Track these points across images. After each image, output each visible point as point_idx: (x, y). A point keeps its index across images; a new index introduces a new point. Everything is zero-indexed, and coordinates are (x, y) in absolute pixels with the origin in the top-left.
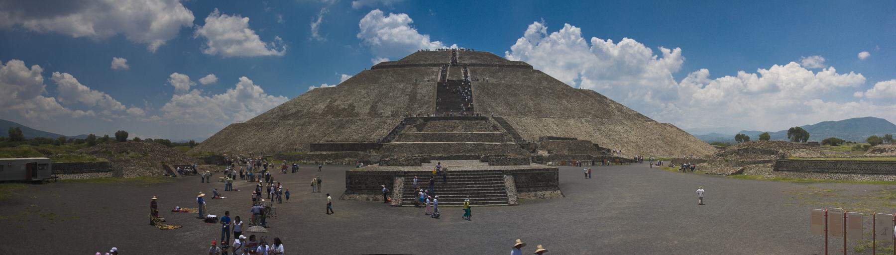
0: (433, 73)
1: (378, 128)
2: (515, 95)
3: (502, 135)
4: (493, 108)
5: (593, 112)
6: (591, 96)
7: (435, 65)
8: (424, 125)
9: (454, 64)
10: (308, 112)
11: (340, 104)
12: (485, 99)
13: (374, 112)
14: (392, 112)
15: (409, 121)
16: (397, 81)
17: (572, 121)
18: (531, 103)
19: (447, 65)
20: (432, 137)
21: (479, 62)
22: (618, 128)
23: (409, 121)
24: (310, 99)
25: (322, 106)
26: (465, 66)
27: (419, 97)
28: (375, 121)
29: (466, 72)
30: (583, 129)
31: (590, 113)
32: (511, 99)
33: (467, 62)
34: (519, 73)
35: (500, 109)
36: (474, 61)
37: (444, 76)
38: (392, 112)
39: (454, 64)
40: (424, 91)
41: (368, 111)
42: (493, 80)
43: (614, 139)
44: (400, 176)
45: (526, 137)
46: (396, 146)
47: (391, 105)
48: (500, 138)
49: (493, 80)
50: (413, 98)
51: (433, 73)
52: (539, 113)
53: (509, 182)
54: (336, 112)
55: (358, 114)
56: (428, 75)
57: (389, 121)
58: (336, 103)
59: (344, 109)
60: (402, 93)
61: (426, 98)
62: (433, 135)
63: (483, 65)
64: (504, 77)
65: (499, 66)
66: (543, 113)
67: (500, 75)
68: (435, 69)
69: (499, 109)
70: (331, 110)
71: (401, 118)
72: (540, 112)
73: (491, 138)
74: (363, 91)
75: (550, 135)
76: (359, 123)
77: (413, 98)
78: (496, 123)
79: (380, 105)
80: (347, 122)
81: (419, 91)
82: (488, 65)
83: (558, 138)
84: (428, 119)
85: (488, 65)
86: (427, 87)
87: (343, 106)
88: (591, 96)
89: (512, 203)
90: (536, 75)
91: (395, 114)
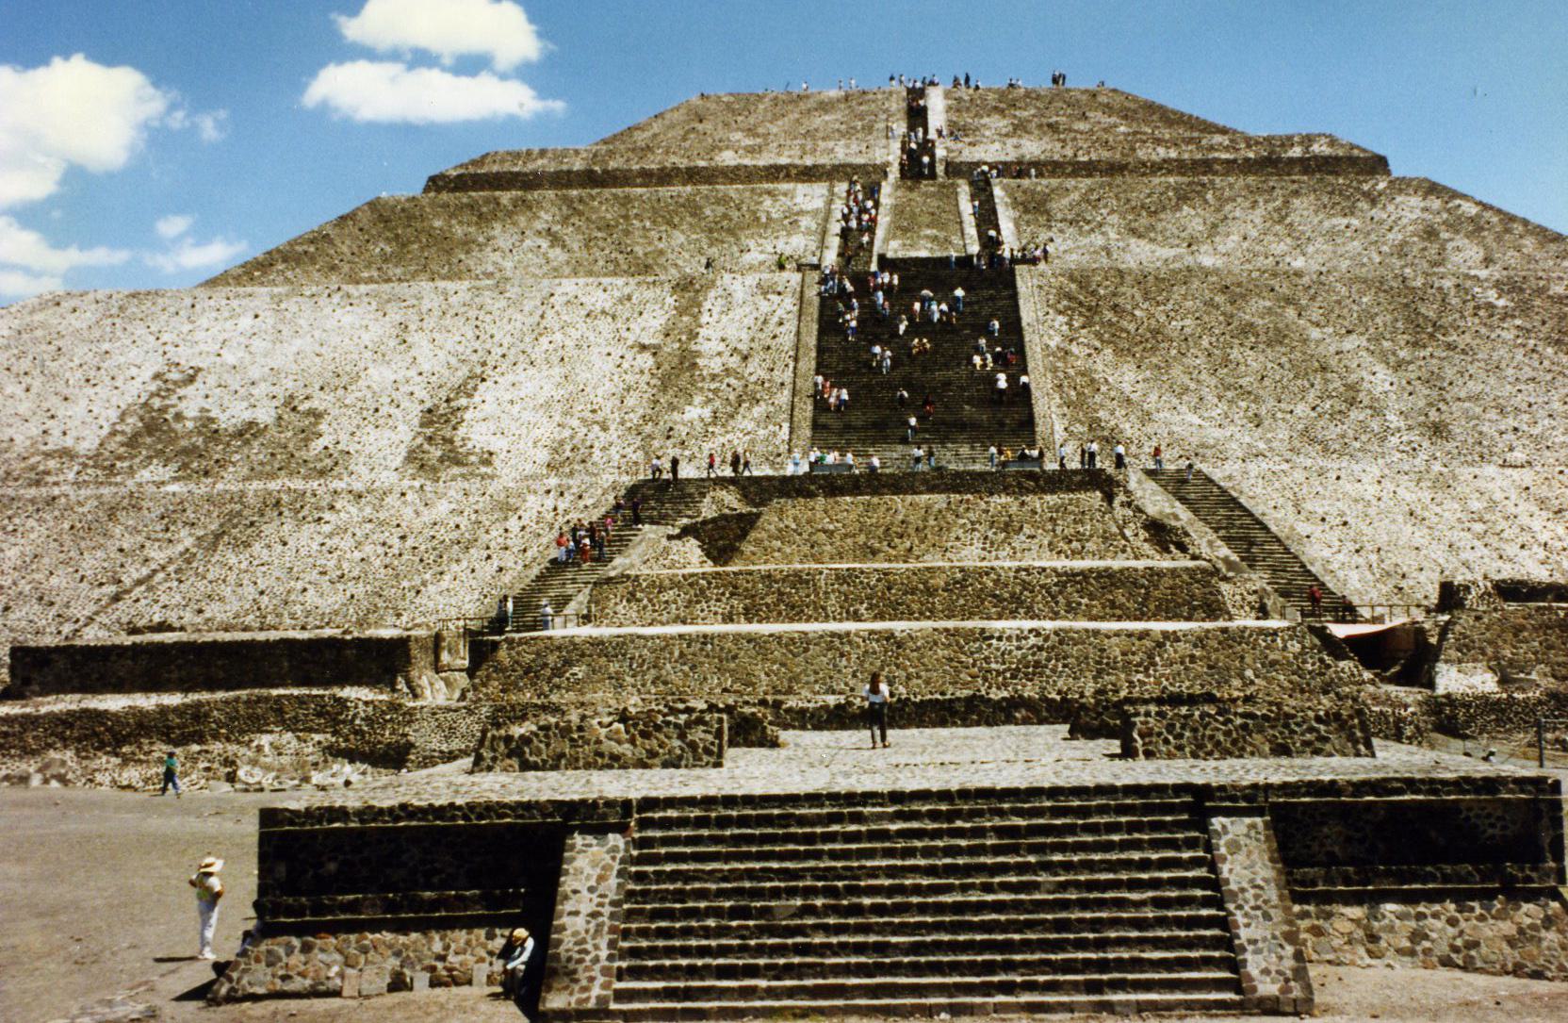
8: (745, 524)
9: (916, 167)
15: (651, 498)
33: (989, 151)
36: (1033, 148)
44: (600, 830)
46: (573, 652)
49: (1140, 254)
50: (677, 370)
51: (791, 220)
53: (1245, 857)
63: (1089, 169)
65: (1180, 167)
67: (1192, 218)
68: (810, 197)
75: (1508, 572)
82: (1114, 169)
84: (762, 491)
85: (1114, 169)
86: (755, 311)
89: (1268, 988)
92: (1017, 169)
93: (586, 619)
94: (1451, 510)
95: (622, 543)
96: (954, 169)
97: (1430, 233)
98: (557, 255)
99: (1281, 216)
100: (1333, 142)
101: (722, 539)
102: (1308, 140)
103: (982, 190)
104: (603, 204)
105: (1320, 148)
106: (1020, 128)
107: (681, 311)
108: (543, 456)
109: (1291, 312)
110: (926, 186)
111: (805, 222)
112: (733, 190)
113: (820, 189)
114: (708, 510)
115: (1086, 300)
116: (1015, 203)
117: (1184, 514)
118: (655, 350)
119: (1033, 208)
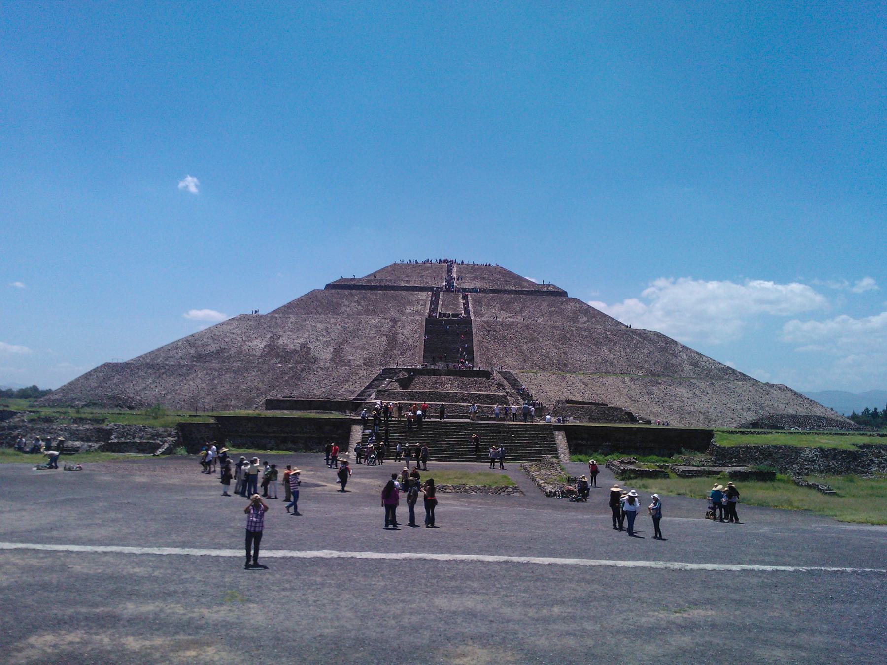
0: (418, 300)
1: (348, 381)
2: (532, 340)
3: (504, 397)
4: (500, 358)
5: (646, 366)
6: (650, 341)
7: (421, 289)
9: (449, 289)
10: (240, 352)
11: (289, 341)
12: (490, 346)
13: (338, 357)
14: (365, 359)
15: (388, 373)
16: (367, 312)
17: (610, 379)
18: (553, 353)
19: (439, 289)
20: (422, 396)
21: (486, 286)
22: (683, 391)
23: (388, 373)
24: (236, 331)
25: (259, 345)
26: (464, 289)
27: (400, 339)
28: (343, 370)
29: (465, 297)
30: (624, 391)
31: (641, 368)
32: (525, 347)
34: (544, 304)
35: (510, 363)
36: (478, 285)
37: (433, 310)
38: (365, 359)
39: (449, 289)
40: (406, 332)
41: (329, 356)
42: (503, 317)
43: (670, 407)
45: (539, 398)
47: (363, 348)
48: (503, 400)
49: (503, 317)
50: (392, 341)
52: (563, 367)
54: (286, 356)
55: (316, 360)
56: (410, 303)
57: (362, 373)
58: (280, 342)
59: (295, 352)
60: (377, 332)
61: (410, 341)
62: (423, 393)
64: (521, 312)
66: (570, 367)
67: (517, 306)
68: (423, 295)
69: (509, 360)
70: (272, 350)
71: (378, 371)
72: (565, 365)
73: (493, 399)
74: (319, 325)
76: (321, 373)
77: (392, 341)
78: (502, 379)
79: (347, 348)
80: (302, 370)
81: (400, 331)
83: (580, 403)
86: (411, 328)
87: (291, 347)
88: (650, 341)
90: (571, 306)
91: (368, 363)
92: (474, 290)
93: (375, 399)
94: (564, 384)
95: (382, 383)
96: (458, 290)
97: (575, 313)
98: (360, 308)
99: (539, 306)
100: (554, 287)
101: (404, 384)
102: (549, 285)
103: (465, 297)
104: (369, 294)
105: (551, 289)
106: (475, 278)
107: (393, 326)
108: (362, 361)
109: (536, 334)
110: (452, 294)
111: (421, 302)
112: (404, 293)
113: (425, 293)
114: (401, 376)
115: (488, 328)
116: (473, 299)
117: (506, 382)
118: (387, 336)
119: (477, 302)
